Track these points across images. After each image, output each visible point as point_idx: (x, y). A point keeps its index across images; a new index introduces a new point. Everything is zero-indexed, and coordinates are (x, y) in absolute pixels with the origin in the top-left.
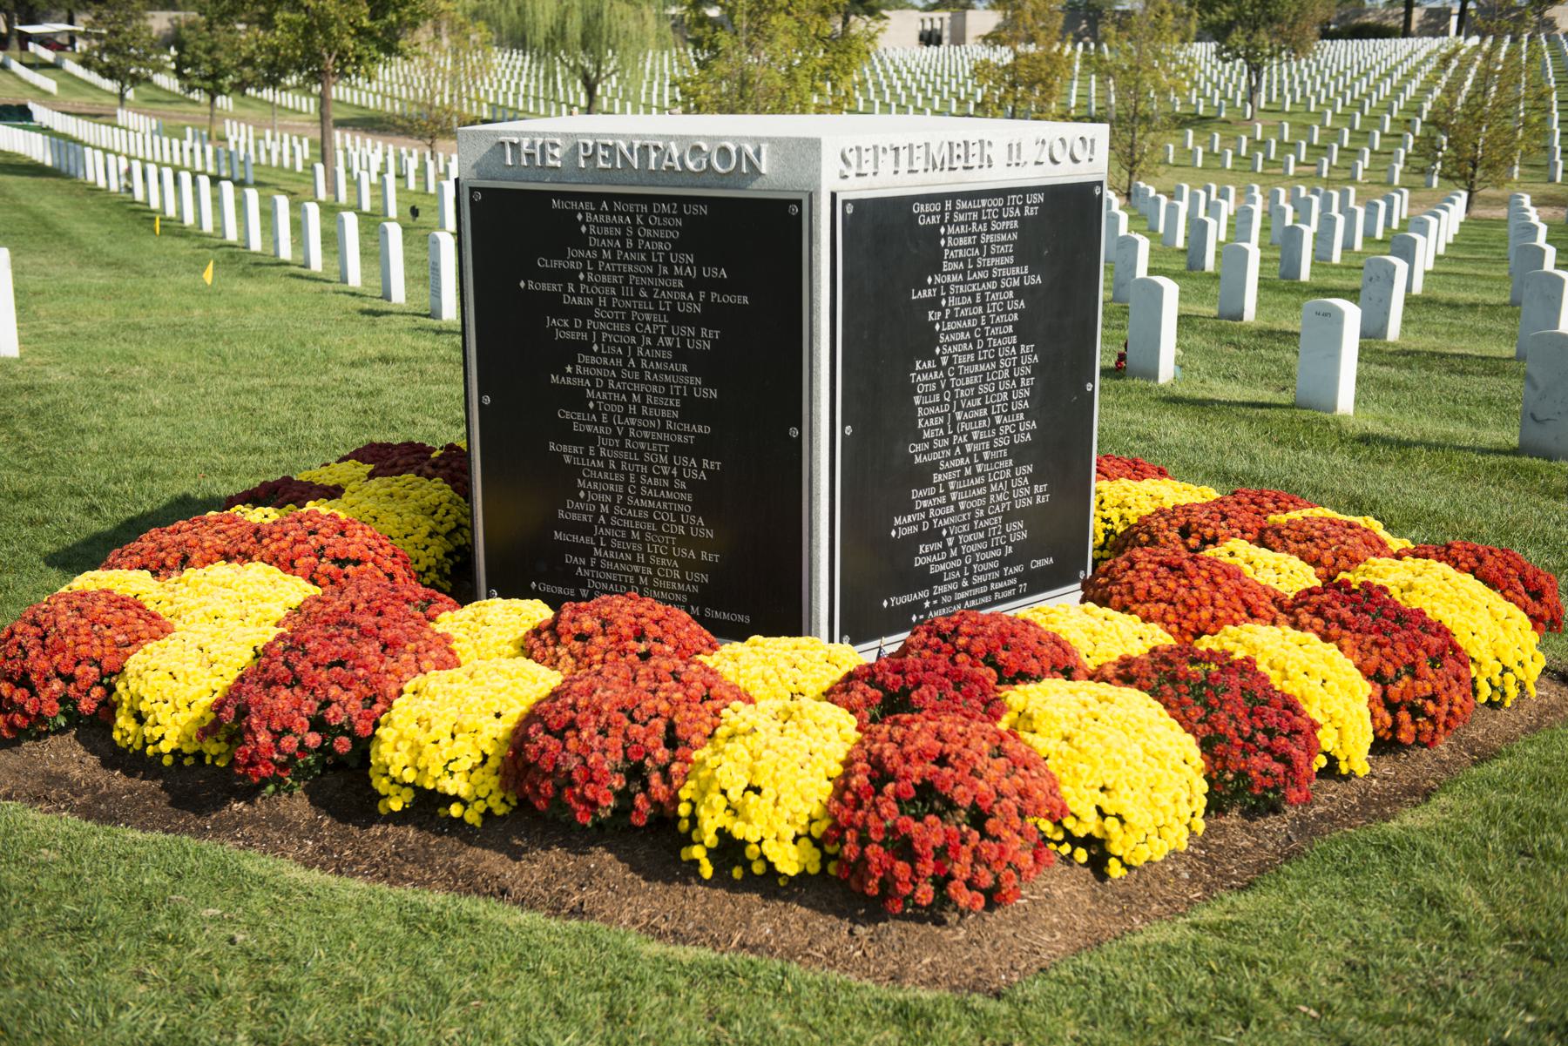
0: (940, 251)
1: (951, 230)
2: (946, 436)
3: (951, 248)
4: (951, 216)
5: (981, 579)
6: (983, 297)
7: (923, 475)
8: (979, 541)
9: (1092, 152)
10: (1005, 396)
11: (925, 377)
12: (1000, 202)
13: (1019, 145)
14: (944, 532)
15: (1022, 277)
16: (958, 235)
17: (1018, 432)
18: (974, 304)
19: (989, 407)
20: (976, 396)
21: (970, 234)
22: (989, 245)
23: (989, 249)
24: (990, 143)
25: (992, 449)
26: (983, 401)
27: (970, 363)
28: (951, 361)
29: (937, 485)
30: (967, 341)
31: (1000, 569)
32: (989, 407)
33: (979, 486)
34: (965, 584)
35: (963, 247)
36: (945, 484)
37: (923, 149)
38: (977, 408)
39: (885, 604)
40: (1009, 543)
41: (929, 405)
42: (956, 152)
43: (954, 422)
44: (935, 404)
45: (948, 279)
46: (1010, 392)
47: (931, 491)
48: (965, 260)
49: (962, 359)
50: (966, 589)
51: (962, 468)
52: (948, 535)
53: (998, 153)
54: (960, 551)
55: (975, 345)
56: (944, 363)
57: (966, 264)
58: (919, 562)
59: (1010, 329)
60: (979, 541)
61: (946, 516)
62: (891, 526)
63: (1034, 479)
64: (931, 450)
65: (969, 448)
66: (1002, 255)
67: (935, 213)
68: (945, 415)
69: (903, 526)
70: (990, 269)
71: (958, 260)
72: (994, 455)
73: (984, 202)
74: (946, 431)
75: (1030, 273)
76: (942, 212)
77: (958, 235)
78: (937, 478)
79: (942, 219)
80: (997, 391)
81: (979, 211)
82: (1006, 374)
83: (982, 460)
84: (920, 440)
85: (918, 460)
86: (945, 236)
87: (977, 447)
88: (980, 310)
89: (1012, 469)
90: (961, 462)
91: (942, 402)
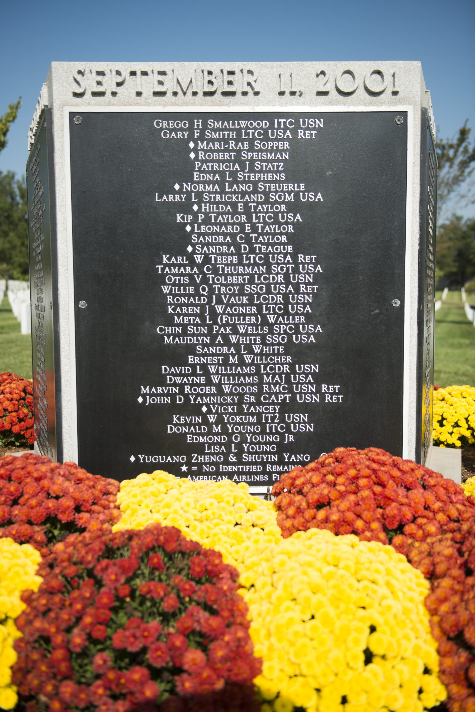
0: (192, 163)
2: (203, 324)
3: (203, 162)
7: (178, 356)
8: (250, 424)
10: (280, 298)
12: (265, 124)
14: (204, 409)
17: (297, 332)
18: (235, 212)
19: (259, 307)
20: (241, 293)
21: (227, 150)
22: (252, 162)
27: (232, 264)
28: (207, 260)
29: (194, 367)
32: (259, 307)
33: (249, 375)
34: (233, 459)
35: (218, 161)
36: (204, 367)
38: (242, 305)
39: (132, 459)
40: (290, 432)
41: (180, 295)
45: (201, 187)
46: (286, 296)
47: (187, 370)
48: (222, 174)
50: (234, 464)
51: (226, 356)
52: (209, 411)
58: (171, 429)
59: (284, 239)
60: (250, 424)
61: (206, 395)
62: (139, 394)
63: (319, 379)
64: (185, 333)
65: (233, 339)
66: (270, 171)
67: (182, 130)
69: (149, 395)
70: (255, 184)
73: (243, 124)
75: (308, 190)
76: (191, 129)
80: (269, 291)
81: (239, 131)
82: (281, 278)
83: (251, 352)
85: (167, 341)
87: (243, 340)
89: (292, 367)
90: (225, 350)
91: (197, 294)
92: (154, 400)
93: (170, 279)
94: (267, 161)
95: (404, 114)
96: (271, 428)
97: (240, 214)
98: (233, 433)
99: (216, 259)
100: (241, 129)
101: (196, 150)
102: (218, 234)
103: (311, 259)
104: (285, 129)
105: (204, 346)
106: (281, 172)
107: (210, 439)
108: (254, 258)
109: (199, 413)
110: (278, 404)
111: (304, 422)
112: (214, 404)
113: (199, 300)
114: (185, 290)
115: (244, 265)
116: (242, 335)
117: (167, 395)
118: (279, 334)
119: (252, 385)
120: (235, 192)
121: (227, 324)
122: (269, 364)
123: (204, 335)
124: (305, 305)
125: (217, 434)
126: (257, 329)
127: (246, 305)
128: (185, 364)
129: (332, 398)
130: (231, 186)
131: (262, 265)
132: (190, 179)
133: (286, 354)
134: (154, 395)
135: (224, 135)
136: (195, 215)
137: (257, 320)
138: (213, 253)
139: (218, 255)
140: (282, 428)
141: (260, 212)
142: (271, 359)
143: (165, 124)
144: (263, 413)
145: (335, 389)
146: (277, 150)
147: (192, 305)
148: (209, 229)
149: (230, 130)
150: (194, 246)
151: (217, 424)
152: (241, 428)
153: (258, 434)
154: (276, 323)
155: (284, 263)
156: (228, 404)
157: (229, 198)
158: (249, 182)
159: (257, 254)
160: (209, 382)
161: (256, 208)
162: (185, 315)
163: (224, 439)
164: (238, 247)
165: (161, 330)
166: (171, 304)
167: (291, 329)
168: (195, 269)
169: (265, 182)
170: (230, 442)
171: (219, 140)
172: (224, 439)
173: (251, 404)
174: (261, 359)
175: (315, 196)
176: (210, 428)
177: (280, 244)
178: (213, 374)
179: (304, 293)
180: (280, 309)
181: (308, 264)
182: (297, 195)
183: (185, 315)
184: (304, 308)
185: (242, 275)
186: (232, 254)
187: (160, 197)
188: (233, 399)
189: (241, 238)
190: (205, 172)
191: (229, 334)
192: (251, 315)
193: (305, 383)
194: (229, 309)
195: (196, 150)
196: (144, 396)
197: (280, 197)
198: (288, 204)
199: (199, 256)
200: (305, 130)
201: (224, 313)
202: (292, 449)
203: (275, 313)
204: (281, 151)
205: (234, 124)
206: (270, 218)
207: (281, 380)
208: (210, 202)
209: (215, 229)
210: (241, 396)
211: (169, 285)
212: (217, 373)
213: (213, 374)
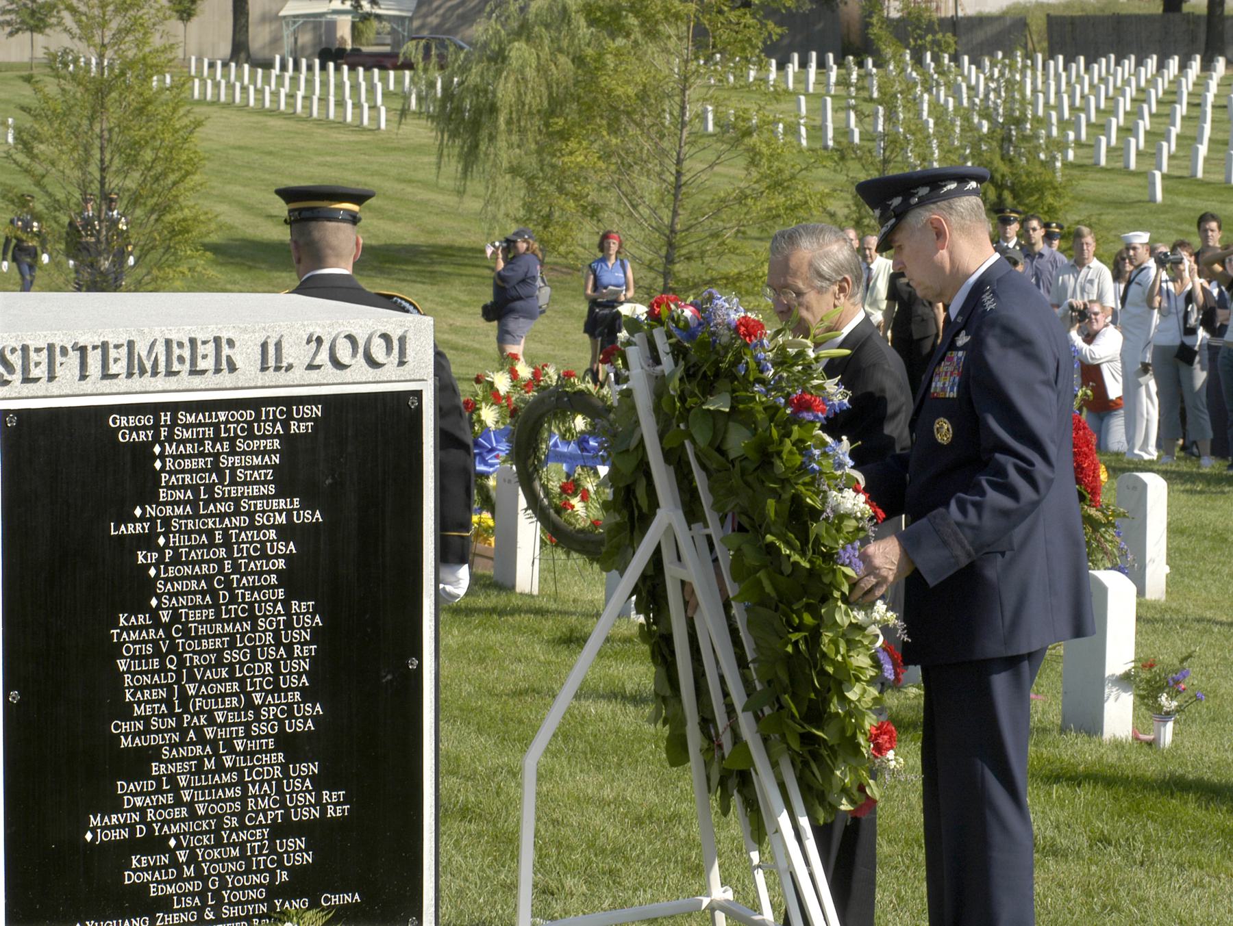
0: (156, 475)
2: (171, 714)
3: (171, 473)
5: (235, 911)
7: (138, 763)
8: (230, 860)
10: (268, 668)
12: (249, 415)
13: (278, 346)
14: (172, 843)
16: (182, 456)
17: (291, 716)
18: (212, 544)
19: (242, 681)
20: (219, 663)
21: (202, 455)
22: (233, 469)
24: (231, 343)
25: (248, 736)
26: (231, 672)
27: (207, 621)
28: (175, 617)
29: (158, 779)
30: (203, 593)
31: (269, 899)
32: (242, 681)
33: (230, 785)
35: (191, 471)
36: (172, 778)
37: (124, 350)
38: (220, 681)
40: (283, 868)
41: (141, 673)
42: (176, 352)
43: (184, 699)
45: (168, 511)
46: (276, 663)
47: (150, 785)
48: (195, 489)
49: (198, 615)
51: (200, 759)
52: (179, 846)
53: (246, 356)
54: (199, 870)
55: (215, 596)
58: (130, 878)
59: (273, 579)
60: (230, 860)
61: (175, 821)
62: (86, 827)
63: (319, 783)
64: (147, 731)
65: (209, 733)
66: (256, 482)
67: (145, 428)
68: (170, 687)
69: (102, 829)
70: (237, 501)
71: (184, 487)
72: (252, 745)
73: (222, 416)
74: (170, 706)
75: (303, 507)
76: (156, 427)
77: (182, 456)
78: (156, 768)
80: (254, 659)
81: (216, 426)
82: (269, 638)
83: (231, 750)
84: (127, 715)
85: (125, 743)
86: (162, 457)
87: (222, 733)
88: (222, 553)
89: (285, 768)
91: (163, 669)
92: (106, 836)
93: (128, 649)
94: (253, 468)
95: (418, 394)
96: (258, 863)
97: (218, 546)
98: (210, 875)
99: (187, 614)
100: (219, 423)
102: (189, 578)
103: (308, 607)
104: (275, 421)
105: (172, 746)
107: (180, 888)
108: (236, 610)
109: (165, 849)
110: (266, 826)
111: (301, 850)
112: (185, 834)
113: (166, 678)
114: (147, 664)
115: (222, 621)
116: (221, 726)
117: (123, 826)
118: (268, 721)
119: (233, 800)
120: (211, 515)
121: (202, 711)
122: (255, 766)
123: (172, 730)
124: (300, 674)
125: (189, 879)
127: (225, 680)
128: (148, 776)
129: (335, 811)
130: (206, 507)
131: (245, 619)
132: (154, 499)
133: (276, 750)
134: (106, 827)
135: (198, 433)
136: (161, 551)
137: (239, 702)
138: (183, 607)
139: (190, 608)
140: (272, 862)
141: (243, 542)
142: (258, 760)
144: (248, 841)
145: (339, 796)
146: (265, 452)
147: (156, 686)
148: (179, 571)
149: (205, 425)
150: (159, 597)
151: (188, 864)
152: (219, 867)
153: (241, 874)
154: (263, 704)
155: (272, 615)
156: (201, 833)
157: (204, 524)
159: (239, 604)
160: (179, 802)
161: (238, 536)
162: (148, 702)
163: (196, 886)
164: (214, 593)
166: (129, 687)
167: (282, 712)
168: (161, 632)
170: (206, 889)
171: (191, 441)
172: (196, 886)
173: (232, 830)
175: (313, 516)
176: (180, 872)
177: (269, 587)
178: (183, 788)
179: (298, 658)
180: (268, 683)
181: (304, 614)
183: (148, 702)
184: (299, 680)
185: (220, 636)
186: (207, 607)
187: (117, 528)
188: (209, 825)
189: (219, 582)
190: (173, 488)
191: (204, 726)
192: (231, 695)
193: (301, 791)
195: (162, 457)
196: (93, 831)
197: (268, 520)
198: (279, 528)
199: (165, 613)
200: (299, 421)
201: (197, 696)
202: (287, 891)
203: (262, 690)
204: (270, 453)
205: (210, 417)
206: (255, 550)
207: (271, 790)
208: (179, 531)
209: (187, 570)
210: (219, 817)
211: (126, 658)
212: (189, 787)
213: (183, 788)
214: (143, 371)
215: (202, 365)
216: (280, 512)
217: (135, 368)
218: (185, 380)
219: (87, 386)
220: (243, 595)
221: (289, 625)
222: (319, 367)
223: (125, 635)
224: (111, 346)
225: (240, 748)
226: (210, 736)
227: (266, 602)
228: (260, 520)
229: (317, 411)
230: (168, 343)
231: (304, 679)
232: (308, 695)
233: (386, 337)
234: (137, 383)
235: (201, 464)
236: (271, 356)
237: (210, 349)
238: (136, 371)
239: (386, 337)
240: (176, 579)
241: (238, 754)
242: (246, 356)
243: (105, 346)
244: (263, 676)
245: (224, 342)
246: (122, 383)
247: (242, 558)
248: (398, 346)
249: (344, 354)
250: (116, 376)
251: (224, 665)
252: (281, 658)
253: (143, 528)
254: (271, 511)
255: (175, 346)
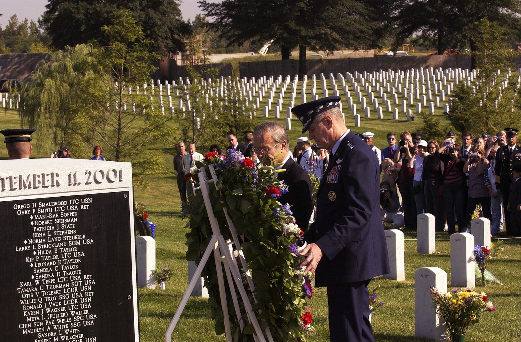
1: (36, 217)
2: (41, 320)
3: (37, 226)
4: (37, 211)
6: (58, 250)
9: (121, 177)
10: (76, 301)
11: (26, 291)
12: (65, 203)
13: (75, 175)
15: (81, 240)
16: (41, 220)
17: (85, 320)
18: (53, 254)
19: (66, 307)
20: (58, 300)
21: (48, 219)
22: (60, 224)
23: (60, 226)
24: (57, 175)
26: (62, 303)
27: (53, 284)
28: (41, 283)
30: (51, 273)
35: (44, 226)
37: (18, 179)
38: (59, 307)
41: (29, 305)
42: (37, 179)
43: (46, 314)
44: (33, 304)
45: (37, 241)
46: (79, 299)
48: (46, 232)
49: (48, 282)
53: (63, 180)
56: (37, 283)
57: (47, 234)
64: (32, 327)
66: (69, 229)
67: (27, 209)
68: (40, 310)
70: (62, 236)
71: (42, 232)
72: (71, 331)
73: (55, 203)
74: (40, 318)
76: (31, 209)
77: (41, 220)
79: (31, 212)
80: (71, 298)
81: (53, 208)
82: (76, 289)
83: (64, 334)
84: (25, 322)
85: (24, 332)
86: (34, 220)
87: (60, 327)
88: (57, 257)
90: (52, 334)
91: (37, 303)
93: (24, 296)
95: (127, 193)
97: (56, 254)
99: (45, 281)
101: (34, 220)
102: (45, 267)
104: (75, 205)
105: (42, 333)
106: (73, 229)
113: (38, 306)
114: (31, 301)
115: (58, 284)
118: (77, 322)
120: (53, 242)
121: (52, 319)
122: (73, 340)
123: (41, 327)
126: (66, 321)
127: (60, 307)
131: (67, 283)
132: (31, 237)
136: (35, 257)
137: (66, 315)
138: (44, 279)
139: (46, 279)
141: (65, 253)
142: (74, 337)
143: (19, 206)
148: (42, 265)
150: (34, 275)
154: (75, 315)
157: (50, 246)
158: (59, 236)
159: (64, 277)
161: (63, 250)
162: (32, 316)
165: (21, 326)
166: (25, 311)
168: (36, 289)
169: (67, 235)
174: (69, 338)
175: (90, 241)
179: (87, 297)
181: (88, 280)
182: (81, 240)
183: (32, 316)
184: (88, 305)
185: (58, 289)
186: (53, 278)
189: (57, 268)
190: (38, 232)
194: (52, 310)
201: (50, 313)
203: (74, 310)
205: (51, 204)
206: (69, 255)
208: (41, 249)
209: (44, 264)
214: (25, 187)
215: (47, 184)
216: (78, 240)
217: (22, 186)
218: (41, 190)
219: (5, 194)
220: (66, 273)
221: (83, 284)
222: (90, 183)
223: (23, 290)
224: (13, 178)
225: (67, 333)
226: (56, 328)
227: (74, 275)
228: (71, 244)
229: (90, 200)
230: (34, 176)
231: (89, 305)
232: (91, 311)
233: (114, 171)
234: (23, 192)
235: (48, 223)
236: (72, 180)
237: (50, 177)
238: (23, 187)
239: (114, 171)
240: (41, 268)
241: (66, 335)
242: (63, 180)
243: (11, 178)
244: (74, 304)
245: (55, 175)
246: (17, 192)
247: (65, 259)
248: (119, 174)
249: (99, 178)
250: (15, 189)
251: (60, 301)
252: (81, 297)
253: (28, 248)
254: (75, 240)
255: (37, 177)
